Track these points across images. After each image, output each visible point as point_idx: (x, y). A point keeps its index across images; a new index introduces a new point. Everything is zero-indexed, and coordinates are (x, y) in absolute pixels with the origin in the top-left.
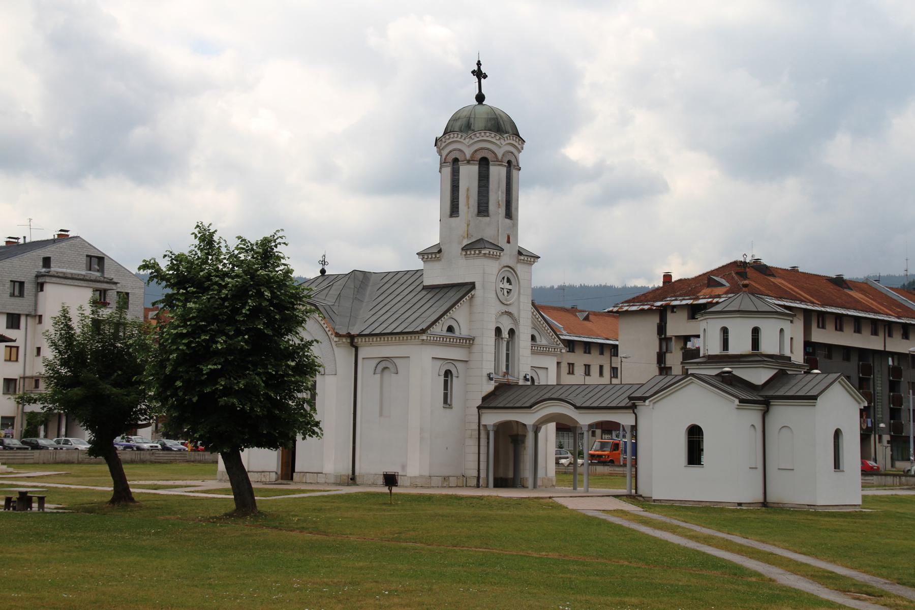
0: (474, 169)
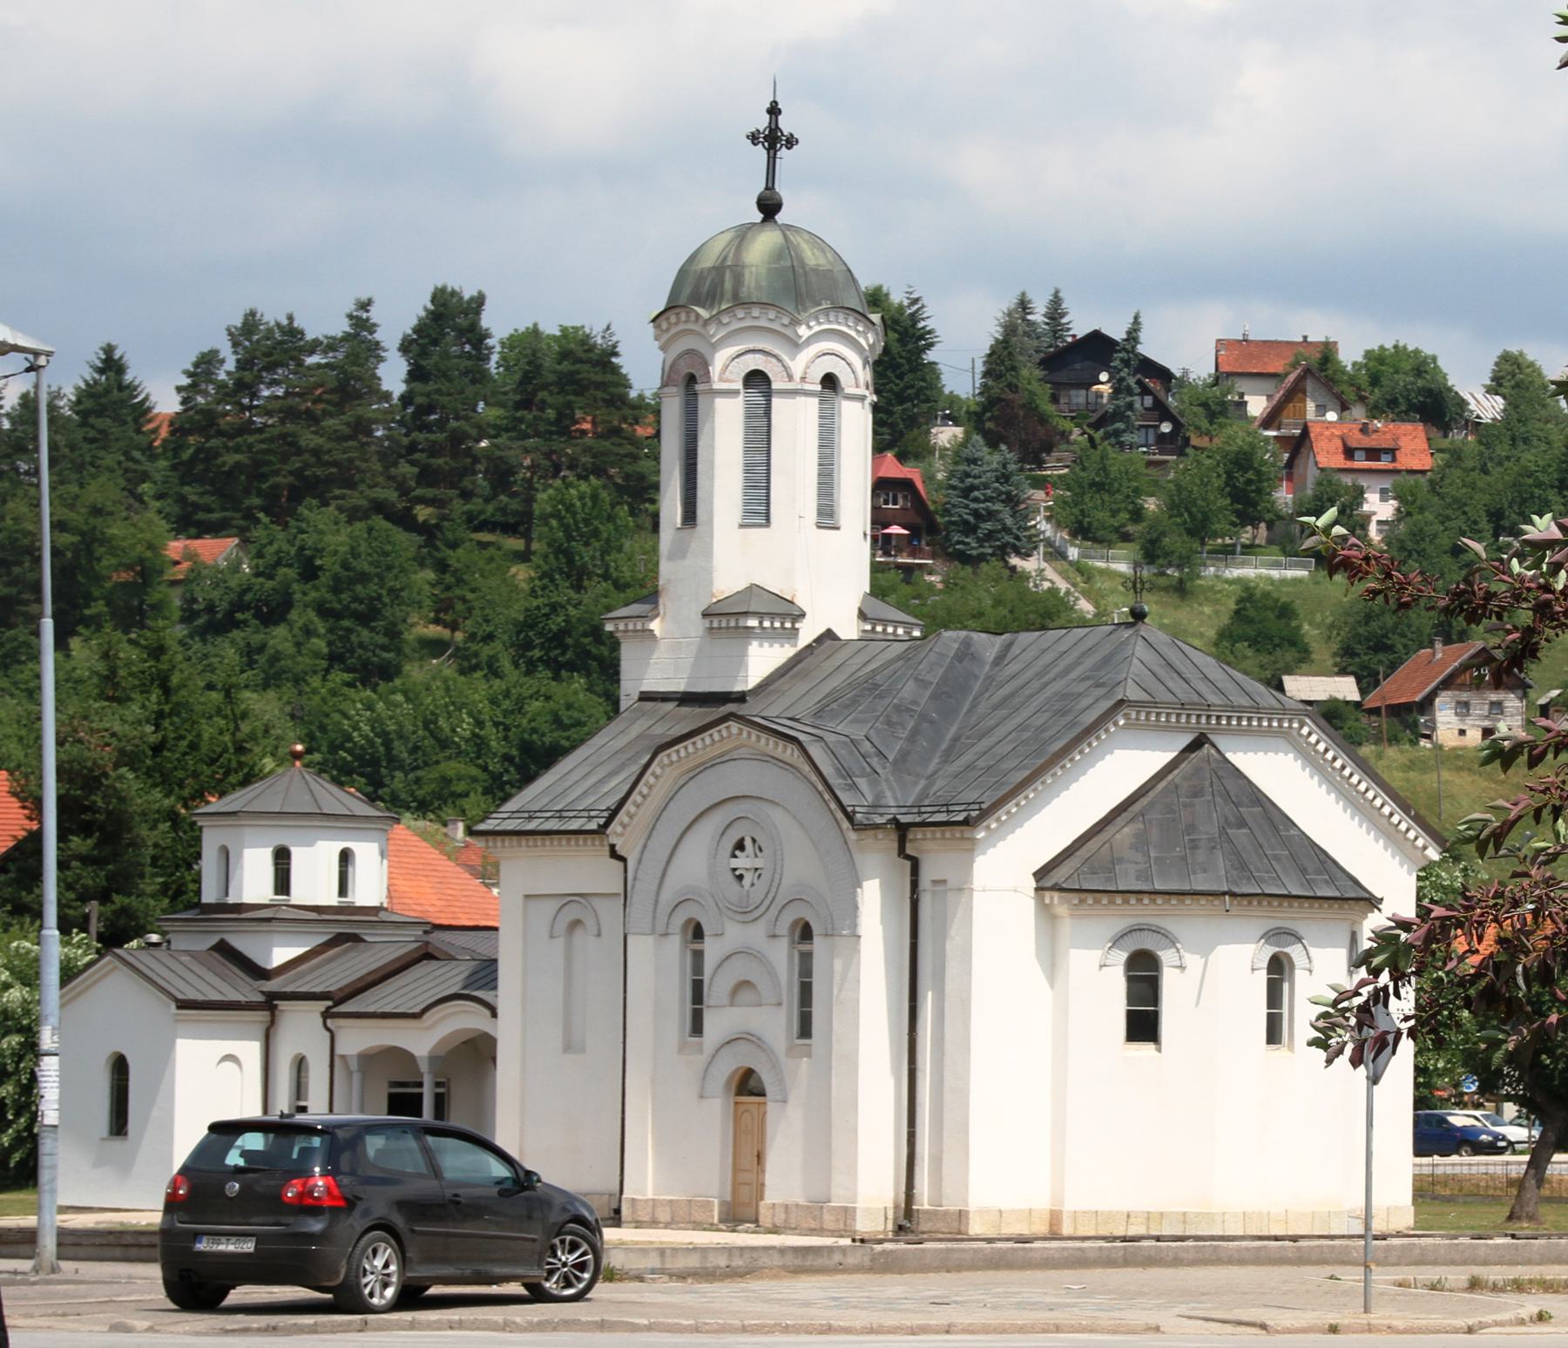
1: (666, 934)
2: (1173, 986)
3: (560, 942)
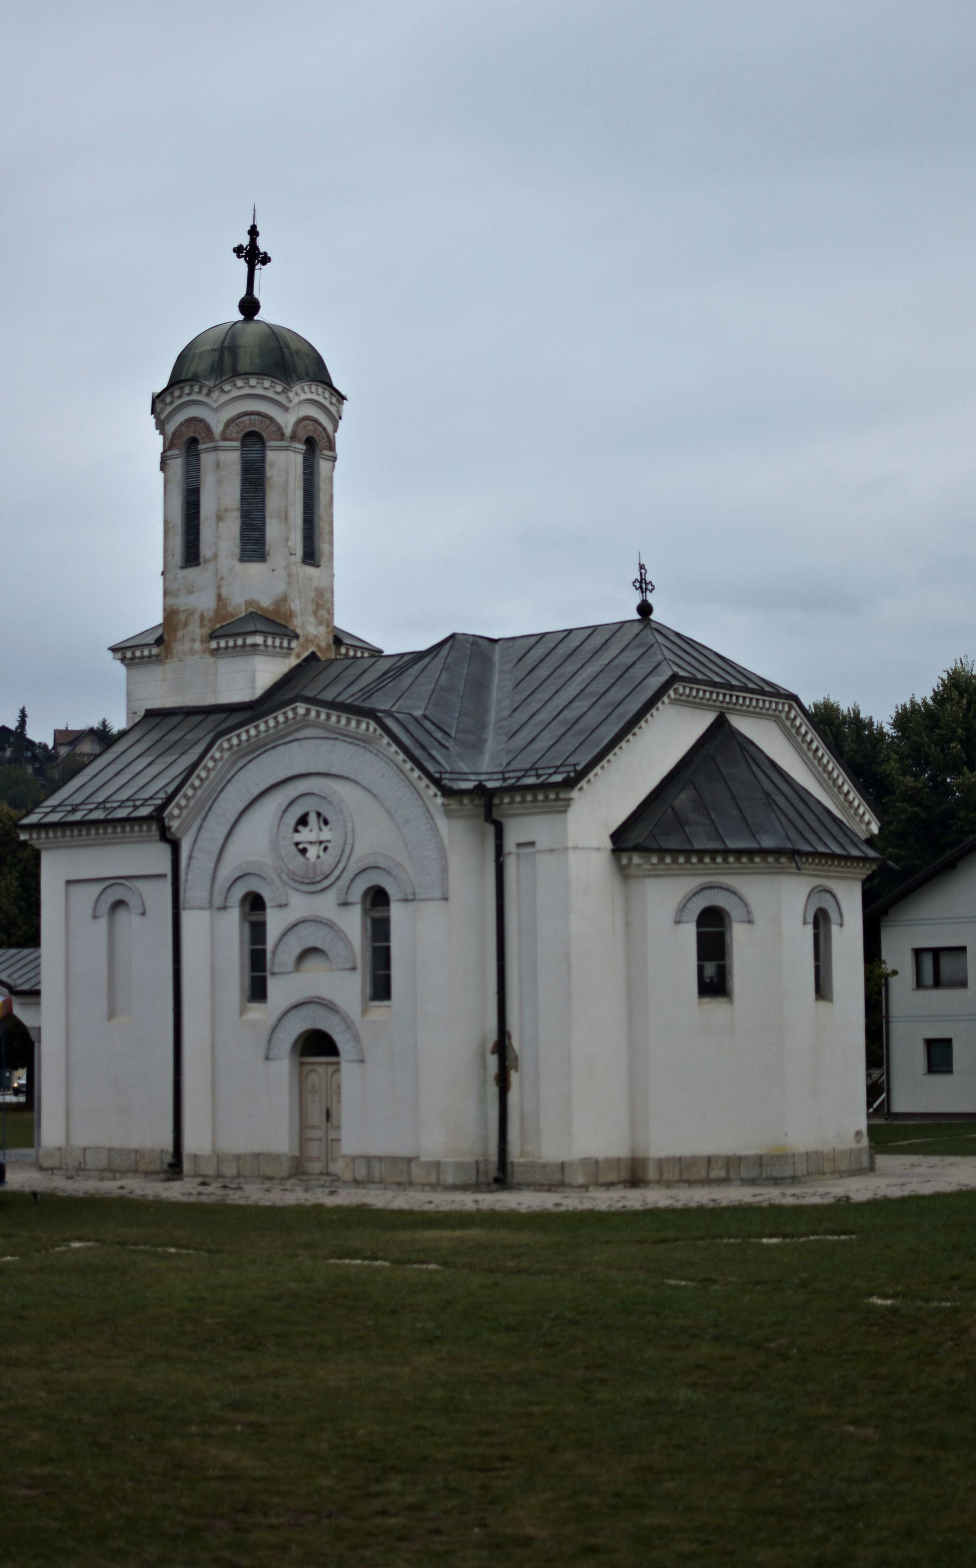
0: (232, 458)
1: (224, 908)
2: (742, 941)
3: (103, 922)
